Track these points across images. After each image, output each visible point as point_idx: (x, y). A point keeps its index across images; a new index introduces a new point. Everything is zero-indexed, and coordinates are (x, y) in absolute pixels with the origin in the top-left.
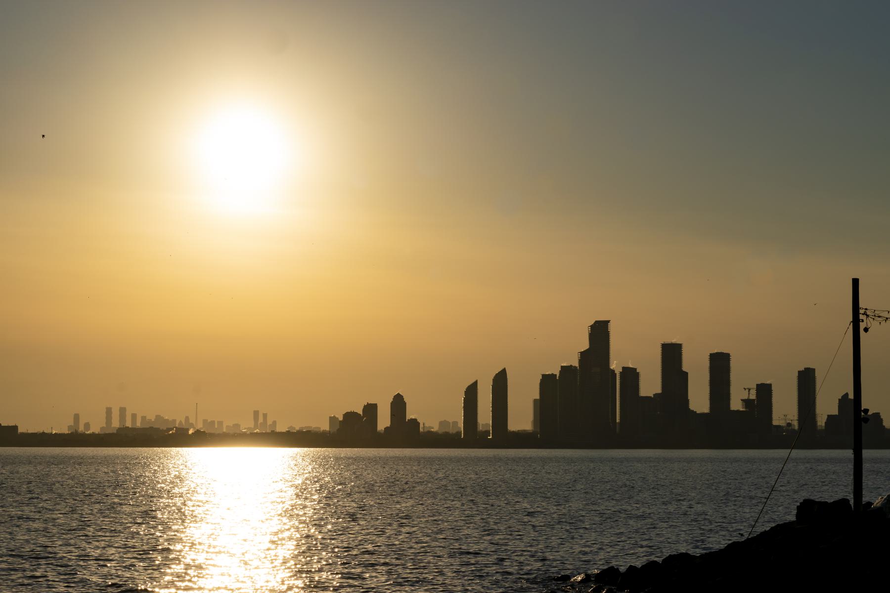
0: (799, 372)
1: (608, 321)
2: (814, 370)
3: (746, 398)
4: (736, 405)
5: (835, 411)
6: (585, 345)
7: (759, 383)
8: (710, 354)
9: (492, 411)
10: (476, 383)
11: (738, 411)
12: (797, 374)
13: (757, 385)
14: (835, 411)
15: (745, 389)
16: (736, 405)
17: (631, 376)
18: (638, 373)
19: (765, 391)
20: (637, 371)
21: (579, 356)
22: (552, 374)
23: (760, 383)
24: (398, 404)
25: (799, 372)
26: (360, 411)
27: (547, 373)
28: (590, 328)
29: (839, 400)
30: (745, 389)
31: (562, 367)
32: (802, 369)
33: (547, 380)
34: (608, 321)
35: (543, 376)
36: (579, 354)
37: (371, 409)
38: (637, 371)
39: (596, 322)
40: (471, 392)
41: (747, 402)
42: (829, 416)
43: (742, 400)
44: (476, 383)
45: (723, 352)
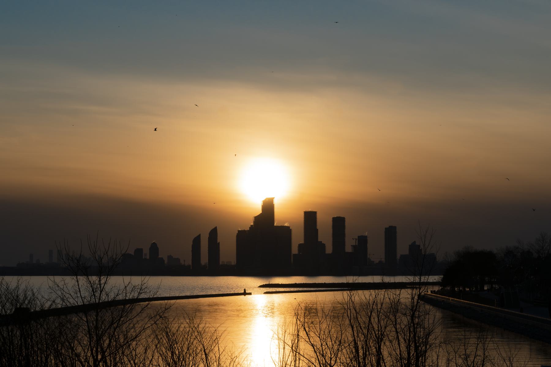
0: (386, 229)
1: (274, 198)
2: (395, 227)
3: (355, 244)
4: (348, 249)
5: (407, 252)
6: (261, 212)
7: (360, 235)
8: (333, 218)
9: (208, 253)
10: (199, 236)
11: (348, 253)
12: (384, 230)
13: (358, 237)
14: (407, 252)
15: (353, 239)
16: (348, 249)
17: (285, 231)
18: (291, 229)
19: (363, 241)
20: (290, 228)
21: (254, 219)
22: (244, 230)
23: (360, 235)
24: (154, 248)
25: (386, 229)
26: (133, 254)
27: (240, 230)
28: (262, 202)
29: (410, 245)
30: (353, 239)
31: (251, 225)
32: (388, 226)
33: (242, 235)
34: (274, 198)
35: (239, 231)
36: (254, 218)
37: (139, 251)
38: (290, 228)
39: (267, 199)
40: (197, 241)
41: (354, 247)
42: (401, 255)
43: (352, 246)
44: (200, 235)
45: (340, 216)
